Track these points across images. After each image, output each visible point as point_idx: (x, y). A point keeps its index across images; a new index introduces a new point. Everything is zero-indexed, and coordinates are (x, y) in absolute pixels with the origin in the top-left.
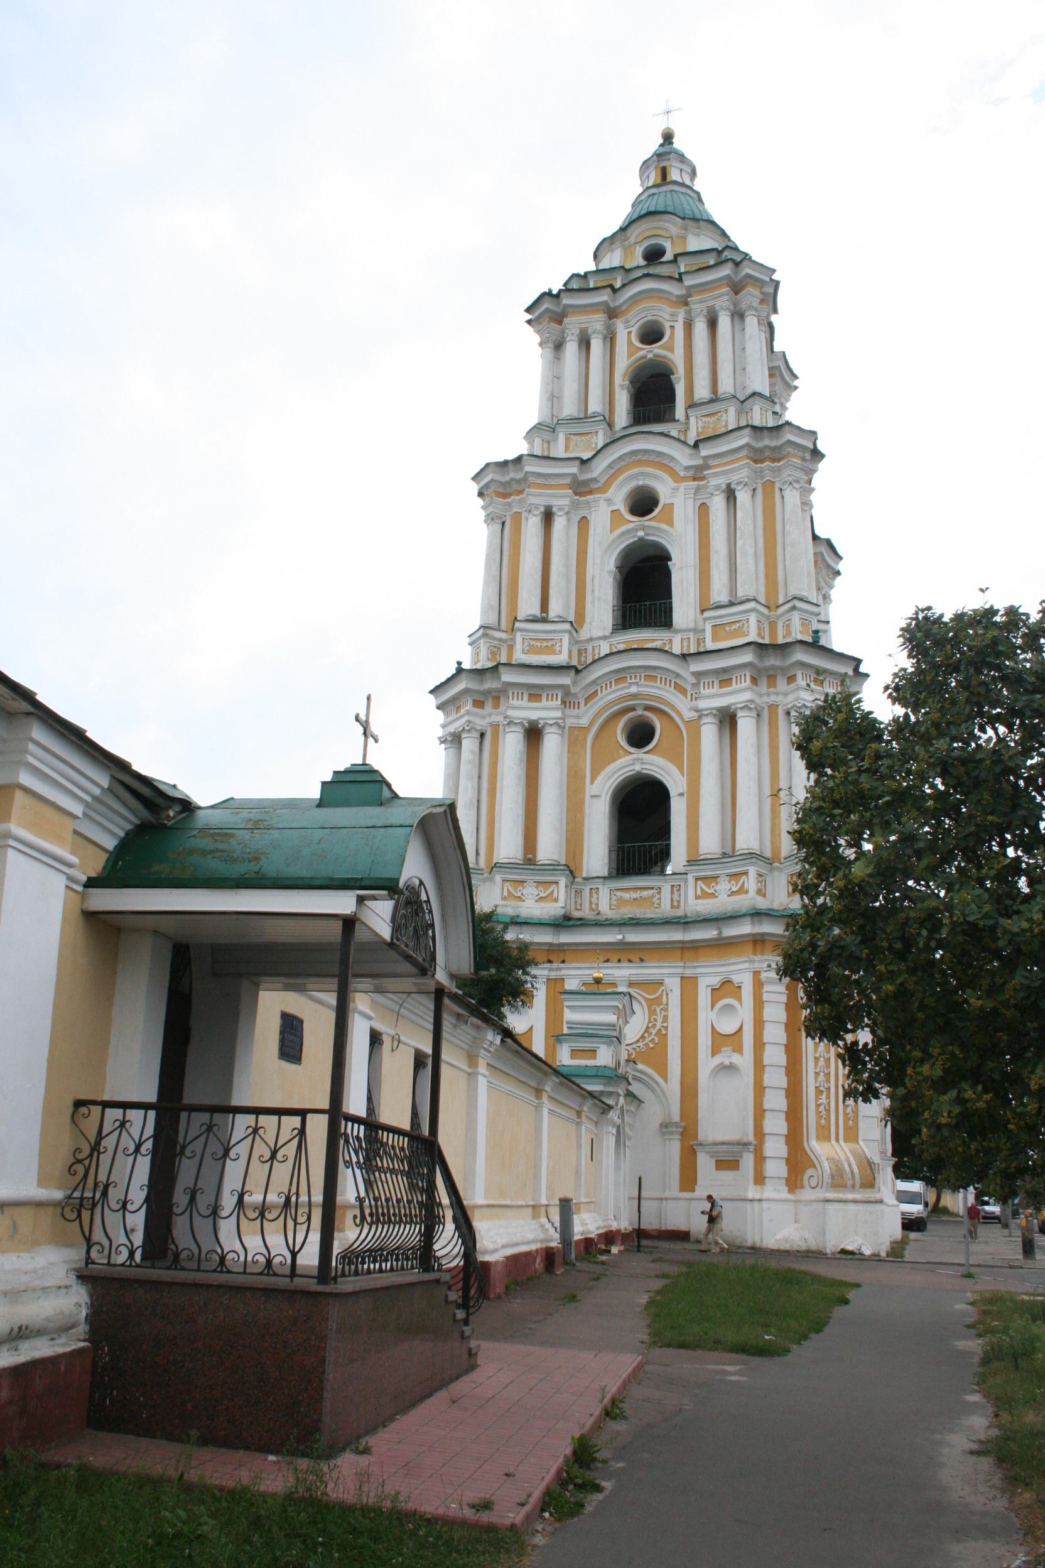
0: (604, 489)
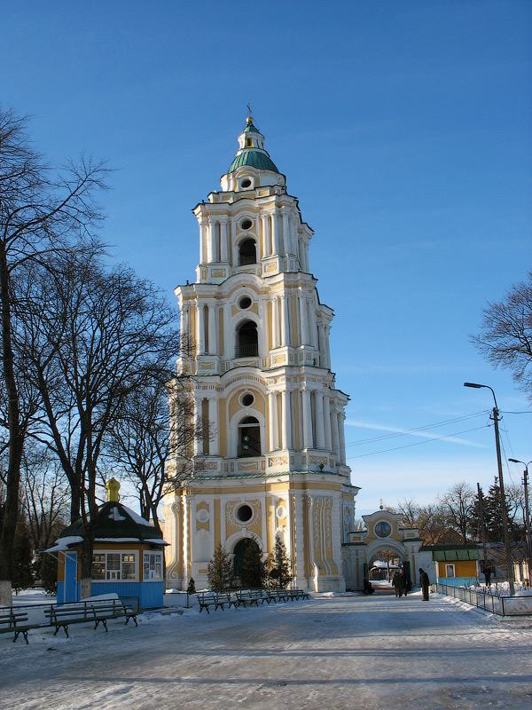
0: (228, 296)
